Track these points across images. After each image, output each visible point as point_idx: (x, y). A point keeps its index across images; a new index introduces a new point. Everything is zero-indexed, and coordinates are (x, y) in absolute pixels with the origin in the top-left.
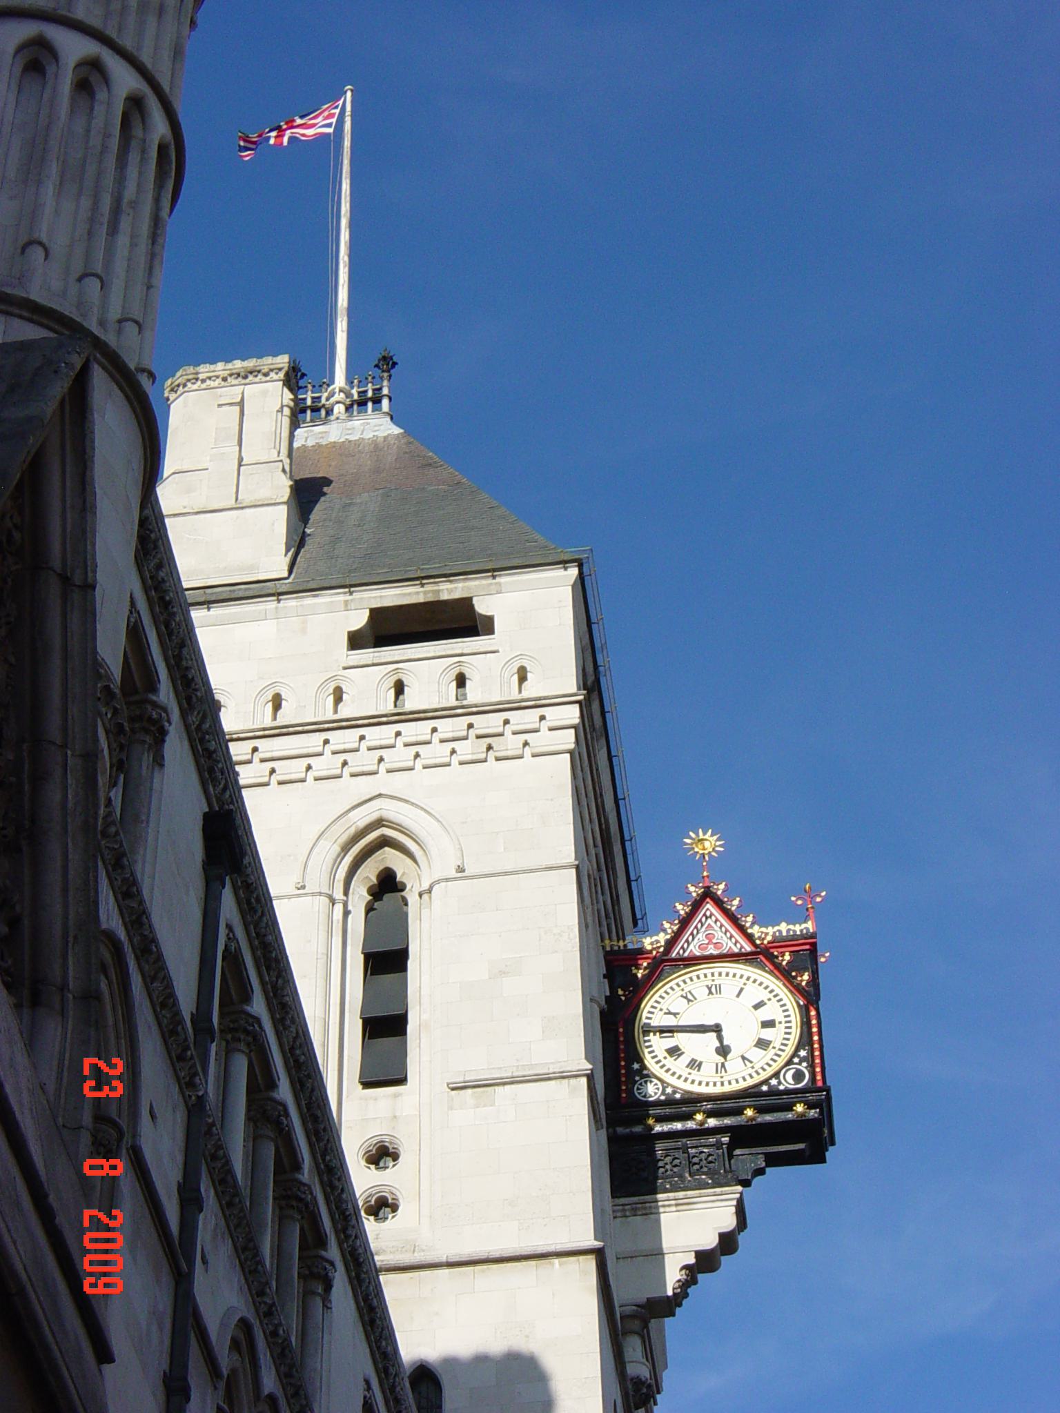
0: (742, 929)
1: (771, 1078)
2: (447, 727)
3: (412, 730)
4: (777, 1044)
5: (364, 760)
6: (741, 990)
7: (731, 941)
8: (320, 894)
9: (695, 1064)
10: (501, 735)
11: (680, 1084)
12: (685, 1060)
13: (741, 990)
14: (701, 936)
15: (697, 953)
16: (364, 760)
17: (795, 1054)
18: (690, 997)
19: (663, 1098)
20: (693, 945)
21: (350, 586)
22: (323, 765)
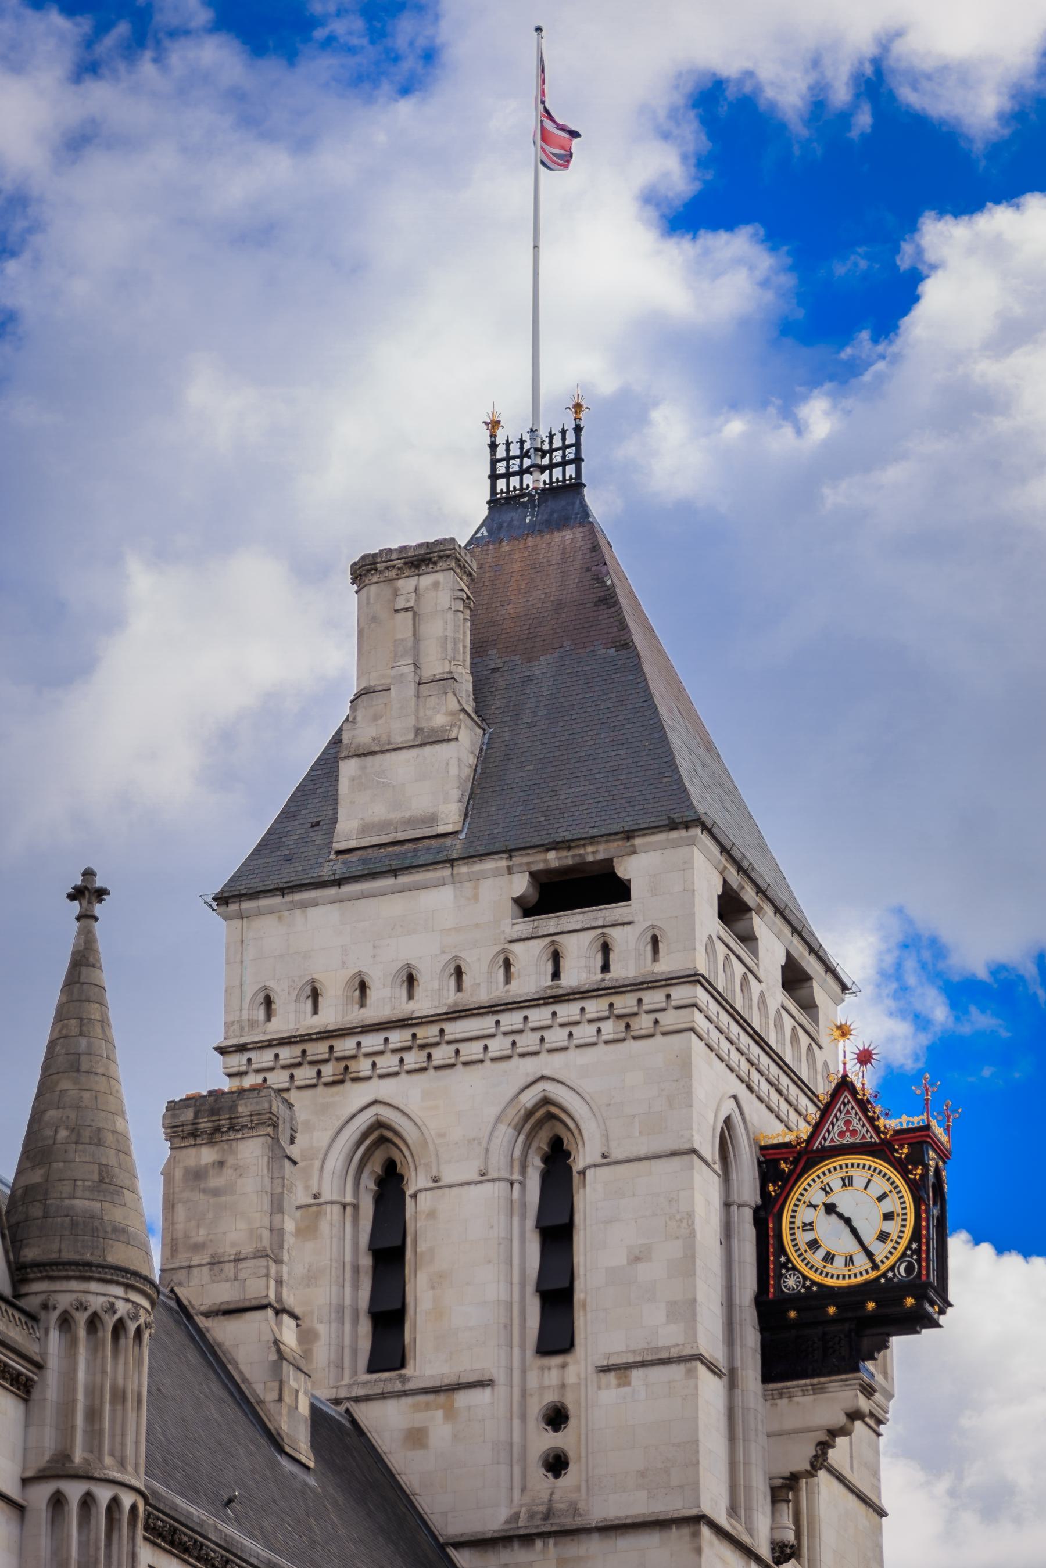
0: (872, 1120)
1: (887, 1271)
2: (595, 1007)
3: (568, 1011)
4: (894, 1236)
5: (528, 1041)
6: (869, 1181)
7: (864, 1133)
8: (499, 1180)
9: (829, 1258)
10: (636, 1014)
11: (816, 1277)
12: (821, 1253)
13: (869, 1181)
14: (840, 1125)
15: (839, 1141)
16: (528, 1041)
17: (908, 1247)
18: (828, 1189)
19: (803, 1290)
20: (833, 1135)
21: (510, 853)
22: (498, 1046)
